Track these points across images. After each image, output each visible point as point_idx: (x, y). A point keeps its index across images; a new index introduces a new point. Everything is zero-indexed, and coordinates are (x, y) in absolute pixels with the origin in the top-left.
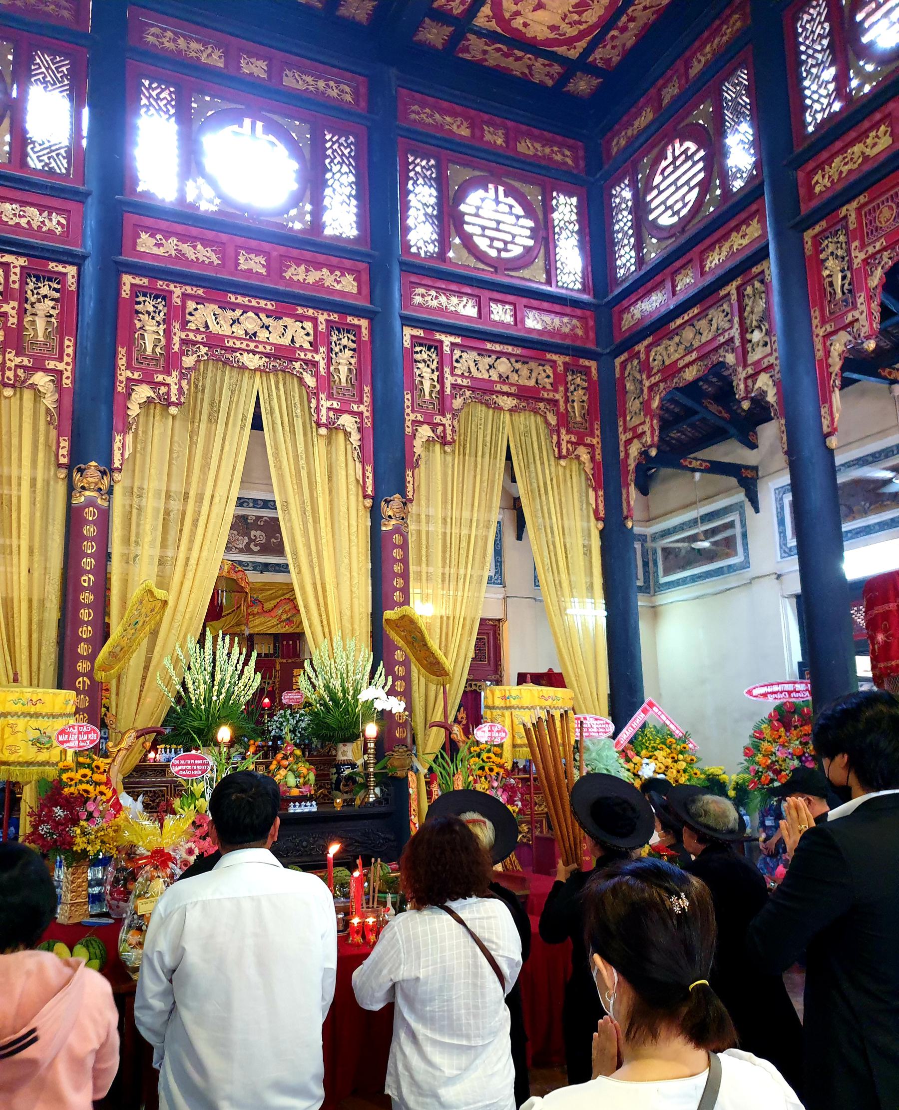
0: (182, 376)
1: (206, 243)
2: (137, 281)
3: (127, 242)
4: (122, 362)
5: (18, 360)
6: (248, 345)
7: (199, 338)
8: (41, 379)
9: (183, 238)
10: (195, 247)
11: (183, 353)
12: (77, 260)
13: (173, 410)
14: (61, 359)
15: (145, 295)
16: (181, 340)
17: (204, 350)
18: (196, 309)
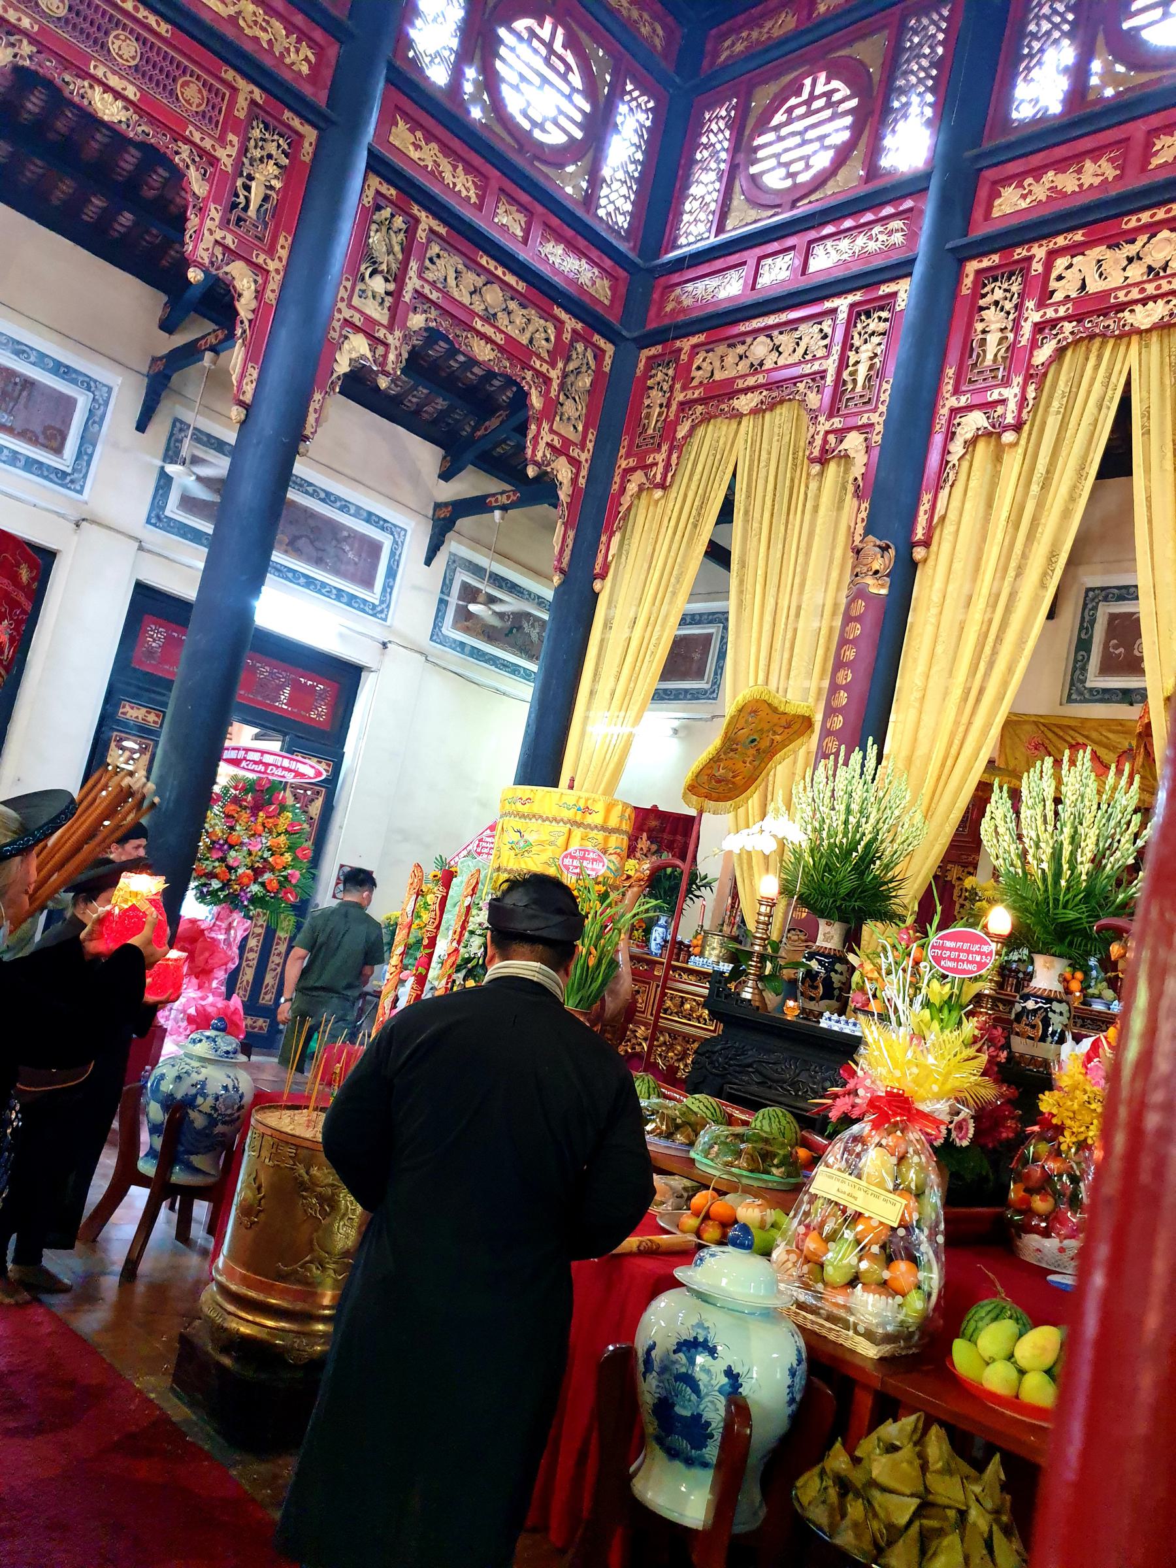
0: (1028, 377)
1: (1095, 154)
2: (986, 263)
3: (978, 214)
4: (948, 387)
5: (827, 426)
6: (1143, 290)
7: (1062, 312)
8: (853, 442)
9: (1060, 166)
10: (1079, 171)
11: (1034, 345)
12: (900, 269)
13: (1009, 437)
14: (874, 410)
15: (995, 280)
16: (1036, 324)
17: (1068, 327)
18: (1070, 266)
